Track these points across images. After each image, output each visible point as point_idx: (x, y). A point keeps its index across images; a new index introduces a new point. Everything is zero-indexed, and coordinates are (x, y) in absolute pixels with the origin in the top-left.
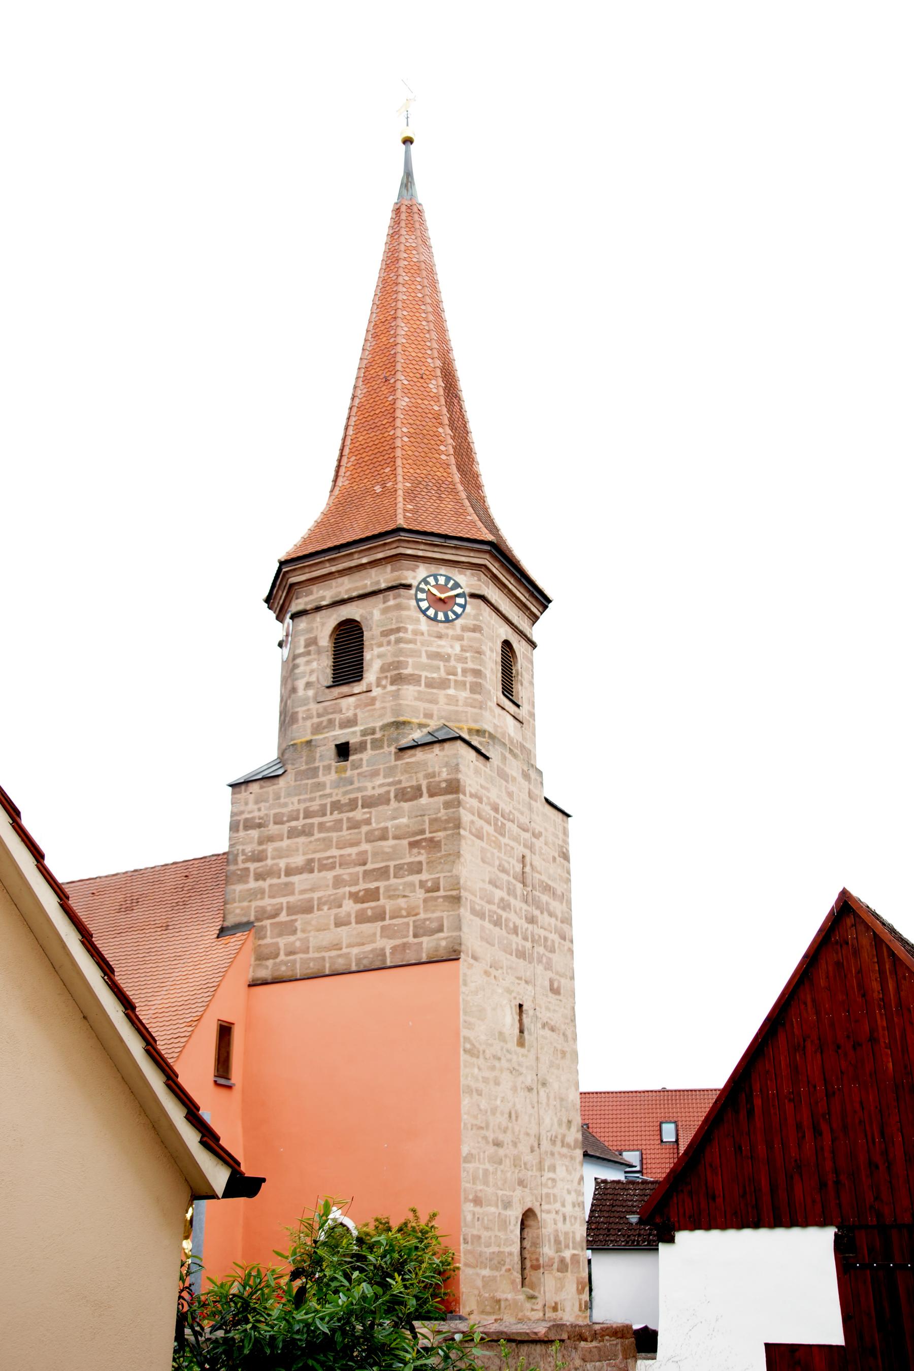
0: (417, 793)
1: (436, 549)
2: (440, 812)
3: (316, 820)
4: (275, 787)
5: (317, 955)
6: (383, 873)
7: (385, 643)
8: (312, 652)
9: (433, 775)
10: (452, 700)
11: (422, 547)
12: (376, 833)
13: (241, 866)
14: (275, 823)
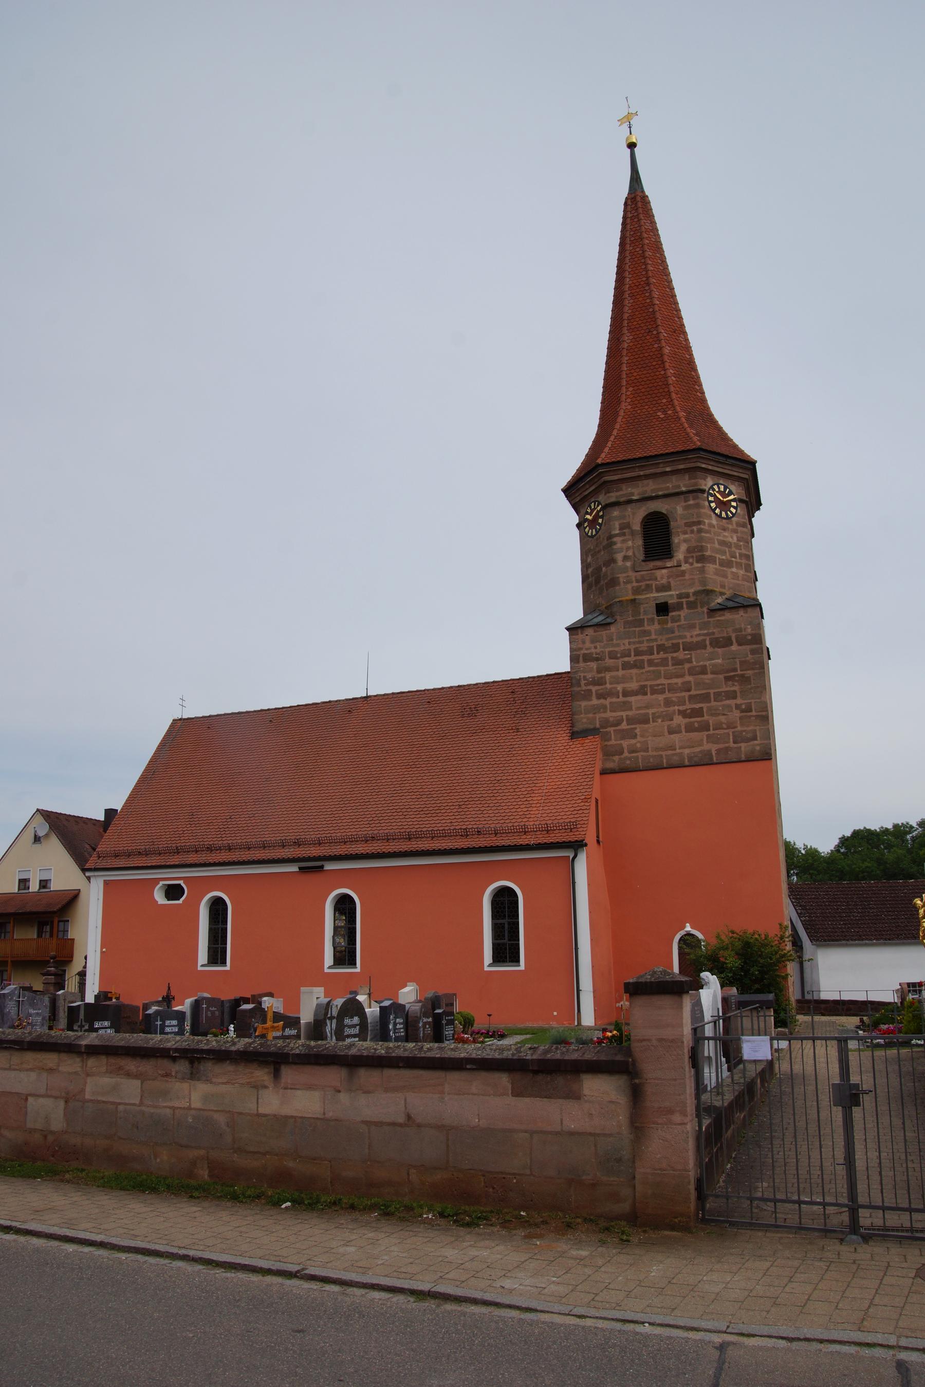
0: (728, 642)
1: (720, 465)
2: (748, 656)
3: (645, 658)
4: (607, 631)
5: (655, 753)
6: (705, 698)
7: (689, 532)
8: (627, 534)
9: (740, 630)
10: (736, 576)
11: (712, 463)
12: (697, 669)
13: (584, 688)
14: (610, 658)
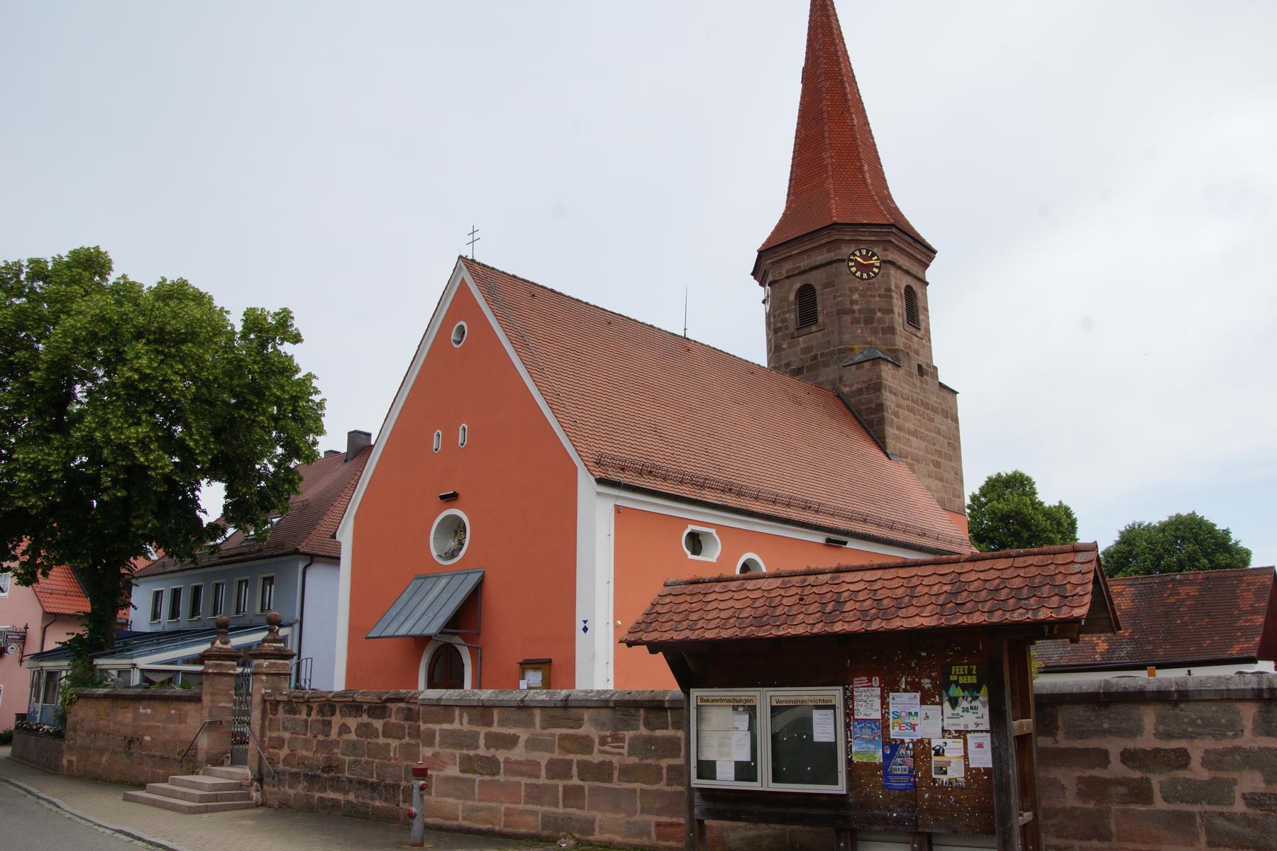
14: (902, 397)
